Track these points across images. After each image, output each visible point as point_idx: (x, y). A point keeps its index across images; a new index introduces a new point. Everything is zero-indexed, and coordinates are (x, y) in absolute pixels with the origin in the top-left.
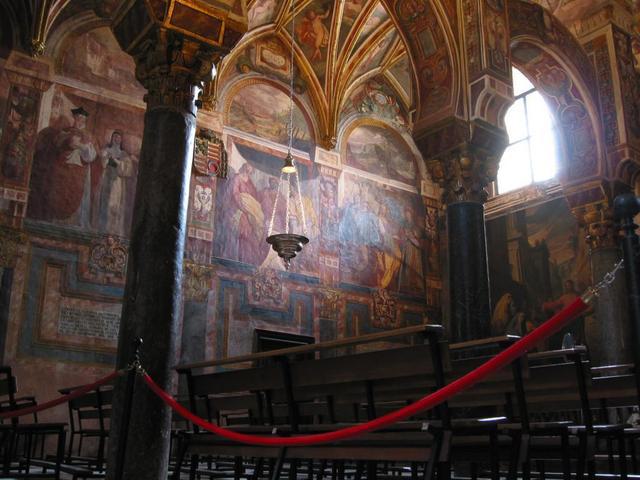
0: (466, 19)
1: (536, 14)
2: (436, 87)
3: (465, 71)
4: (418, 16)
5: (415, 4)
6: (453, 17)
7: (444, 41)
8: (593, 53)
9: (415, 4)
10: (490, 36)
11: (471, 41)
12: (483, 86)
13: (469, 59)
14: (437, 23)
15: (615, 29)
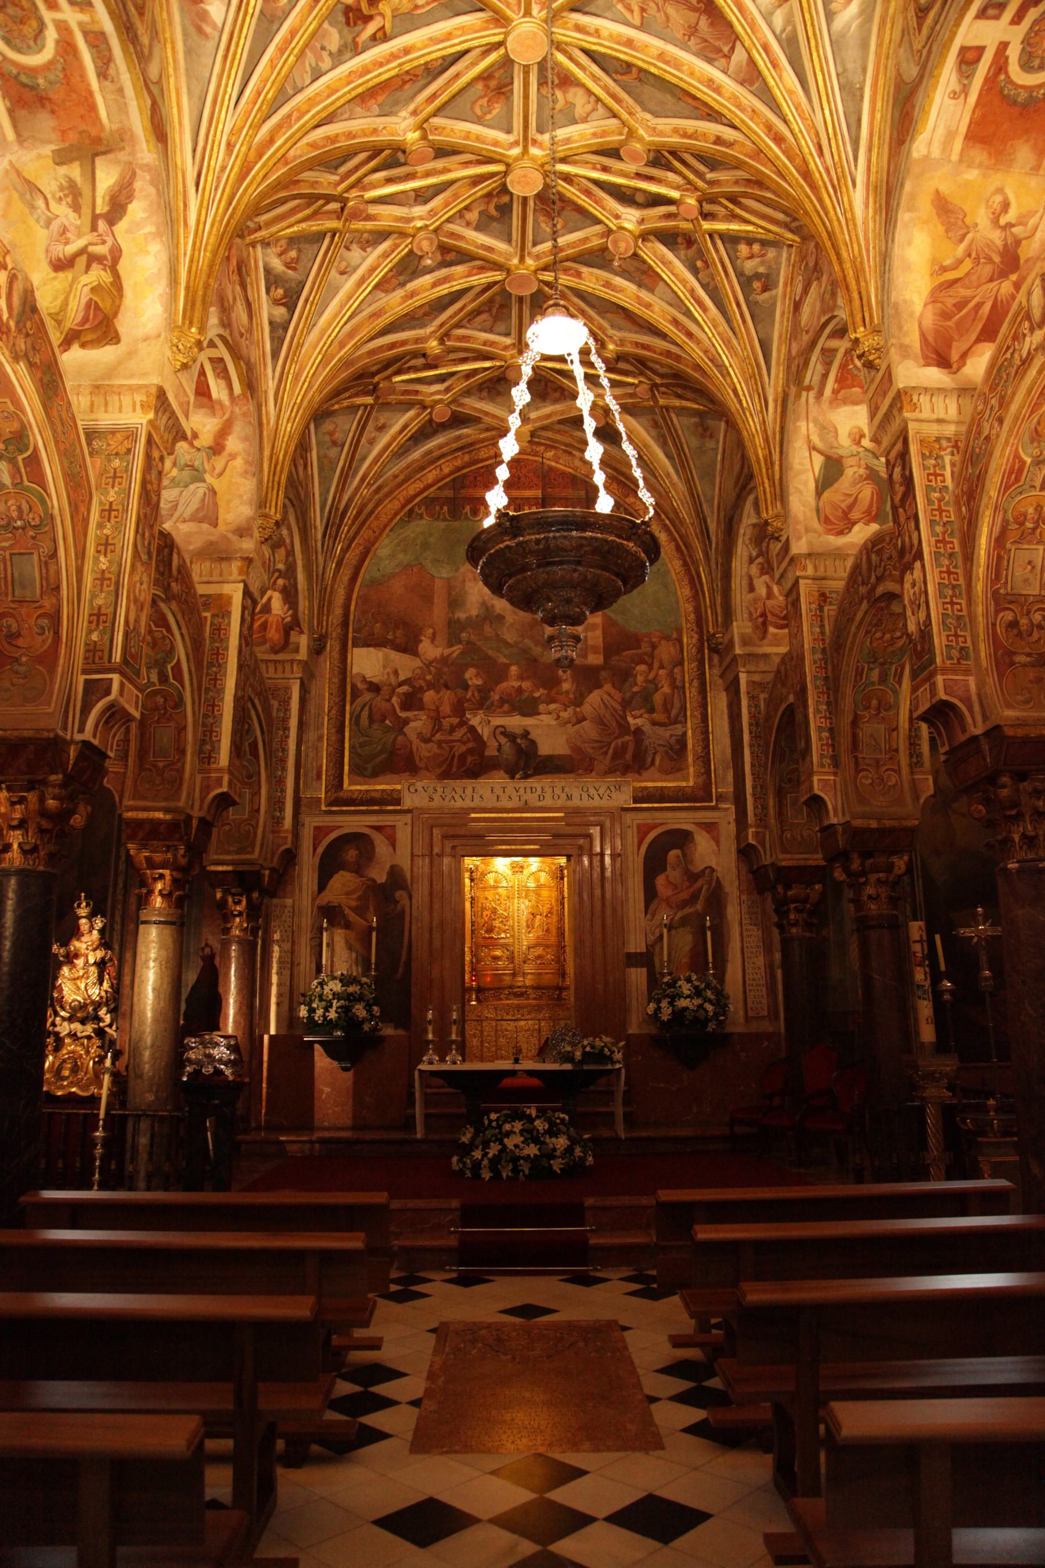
0: (96, 561)
1: (166, 550)
2: (24, 659)
3: (80, 651)
4: (24, 528)
5: (25, 507)
6: (81, 555)
7: (57, 588)
8: (208, 615)
9: (25, 507)
10: (132, 606)
11: (99, 601)
12: (108, 692)
13: (90, 632)
14: (54, 555)
15: (247, 593)
